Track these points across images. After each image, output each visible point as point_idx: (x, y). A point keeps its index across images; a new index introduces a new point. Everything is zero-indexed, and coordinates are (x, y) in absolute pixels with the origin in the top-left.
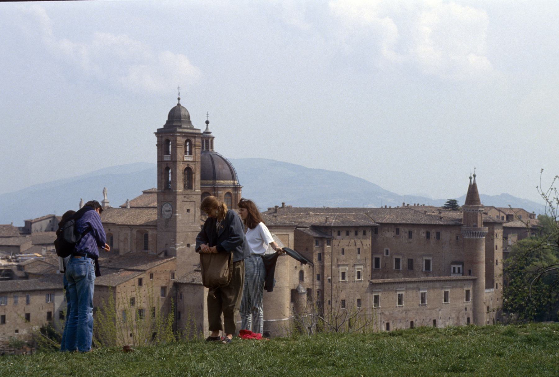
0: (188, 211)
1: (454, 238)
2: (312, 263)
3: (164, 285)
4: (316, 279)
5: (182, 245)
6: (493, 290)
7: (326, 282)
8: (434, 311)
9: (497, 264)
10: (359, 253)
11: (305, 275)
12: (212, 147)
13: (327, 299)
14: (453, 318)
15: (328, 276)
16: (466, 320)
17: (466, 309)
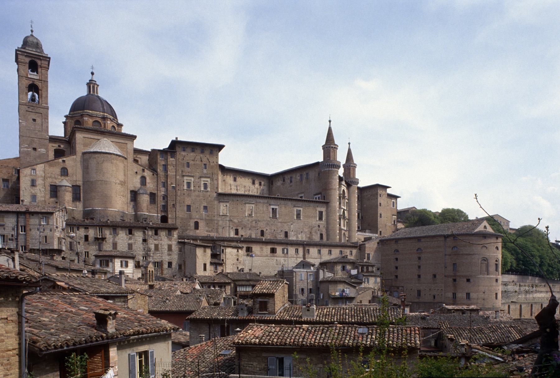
0: (34, 120)
1: (317, 175)
2: (157, 172)
3: (6, 178)
4: (160, 186)
5: (26, 148)
6: (377, 235)
7: (170, 188)
8: (285, 225)
9: (381, 217)
10: (206, 168)
11: (148, 180)
12: (94, 91)
13: (170, 203)
14: (306, 232)
15: (172, 184)
16: (319, 235)
17: (319, 226)
